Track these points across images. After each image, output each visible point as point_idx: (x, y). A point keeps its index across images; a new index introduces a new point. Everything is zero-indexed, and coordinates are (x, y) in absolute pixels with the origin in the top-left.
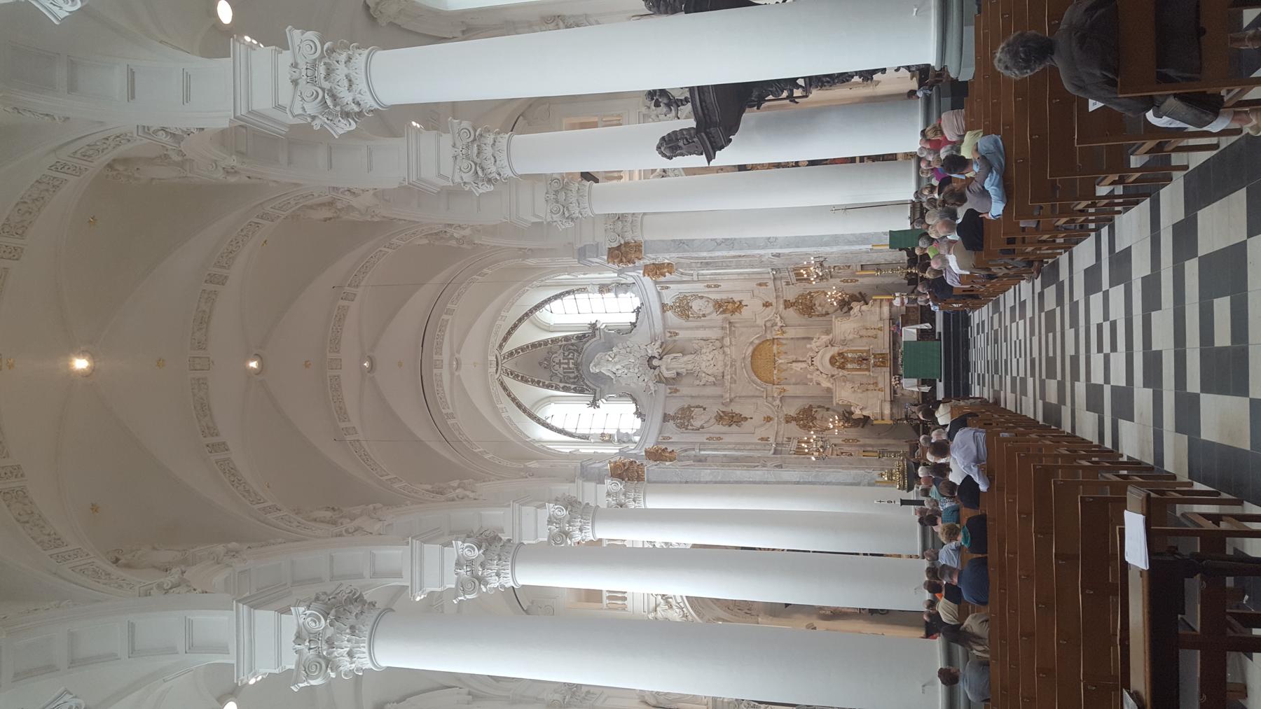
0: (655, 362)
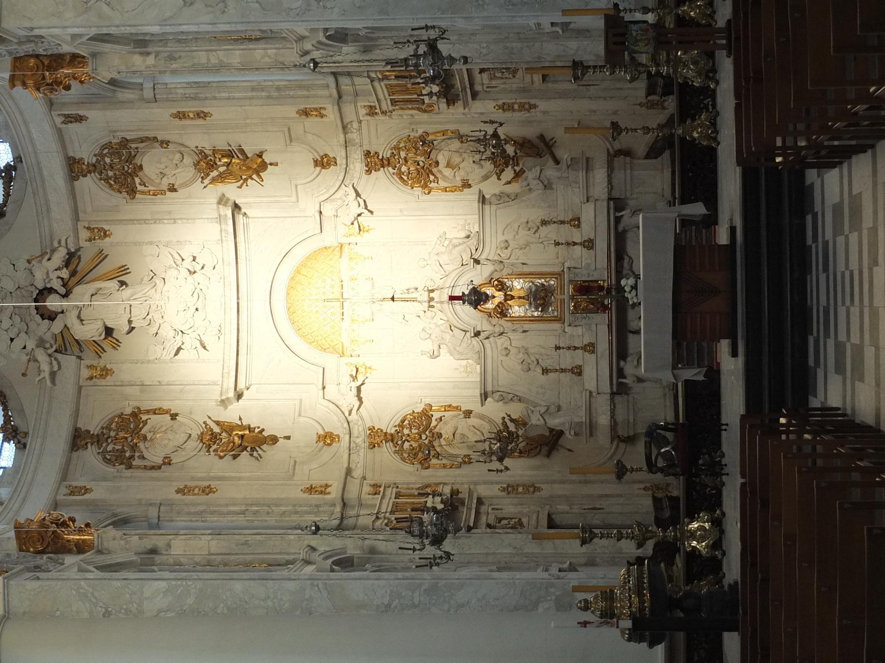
0: (53, 303)
